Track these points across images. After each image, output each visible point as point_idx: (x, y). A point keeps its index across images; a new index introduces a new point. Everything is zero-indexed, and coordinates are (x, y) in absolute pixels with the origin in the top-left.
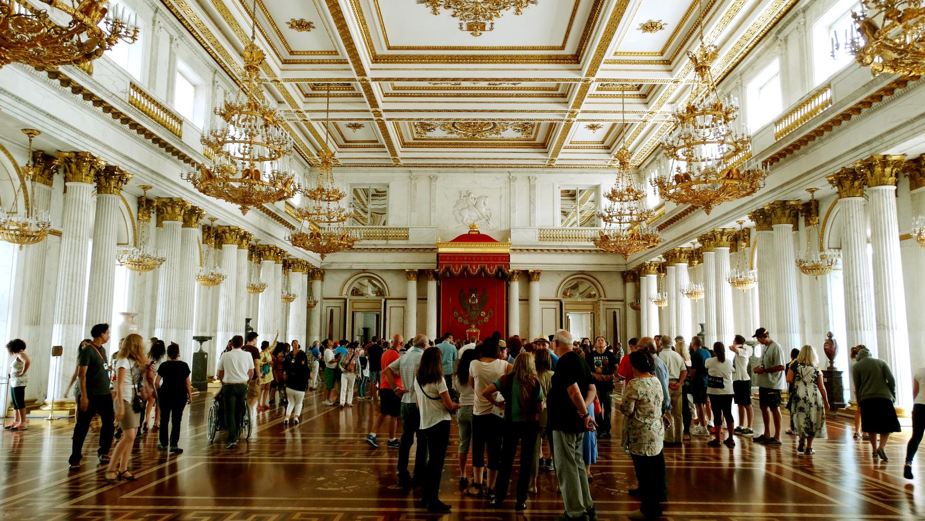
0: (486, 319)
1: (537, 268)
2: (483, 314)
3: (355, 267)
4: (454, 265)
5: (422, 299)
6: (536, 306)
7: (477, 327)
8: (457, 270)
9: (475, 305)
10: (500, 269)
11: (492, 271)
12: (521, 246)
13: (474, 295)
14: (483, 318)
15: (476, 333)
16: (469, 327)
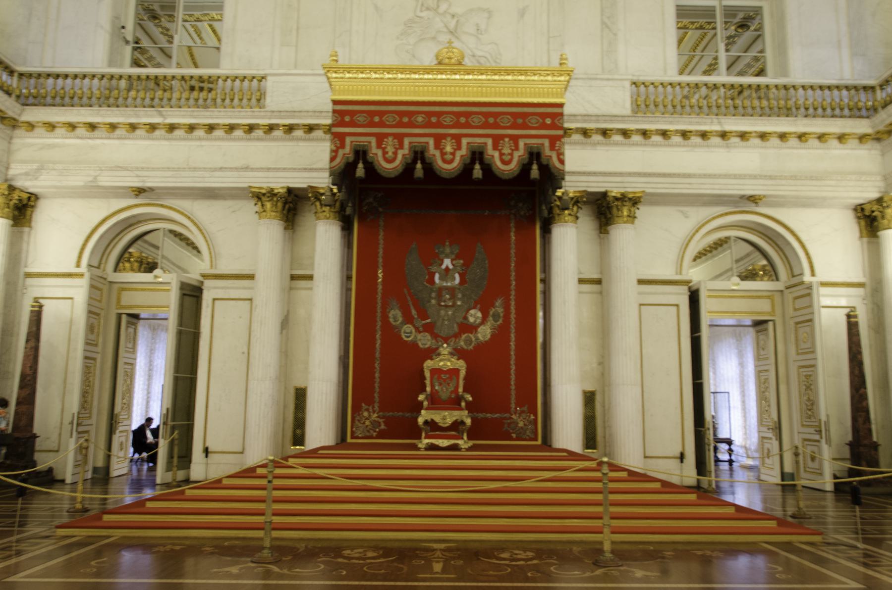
0: (485, 333)
1: (633, 187)
2: (475, 316)
3: (106, 180)
4: (380, 139)
5: (298, 278)
6: (626, 294)
7: (459, 353)
8: (390, 160)
9: (452, 291)
10: (535, 155)
11: (506, 162)
12: (587, 117)
13: (447, 263)
14: (473, 328)
15: (456, 372)
16: (431, 353)
